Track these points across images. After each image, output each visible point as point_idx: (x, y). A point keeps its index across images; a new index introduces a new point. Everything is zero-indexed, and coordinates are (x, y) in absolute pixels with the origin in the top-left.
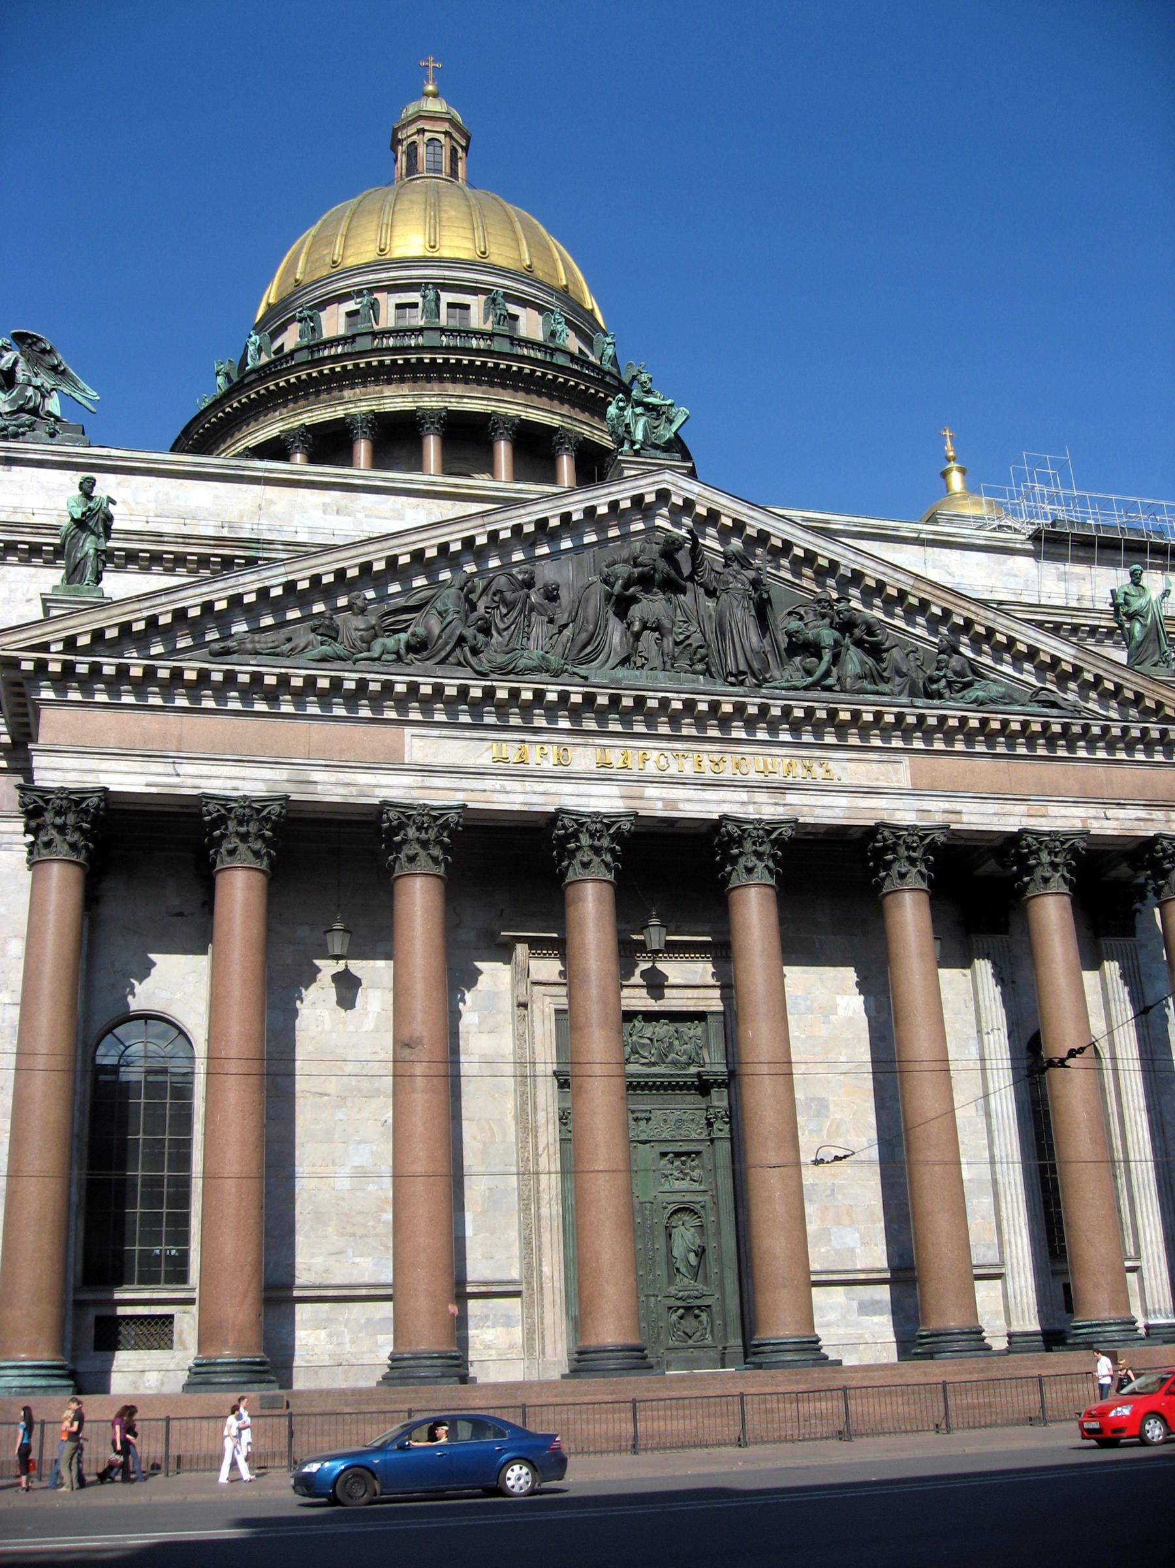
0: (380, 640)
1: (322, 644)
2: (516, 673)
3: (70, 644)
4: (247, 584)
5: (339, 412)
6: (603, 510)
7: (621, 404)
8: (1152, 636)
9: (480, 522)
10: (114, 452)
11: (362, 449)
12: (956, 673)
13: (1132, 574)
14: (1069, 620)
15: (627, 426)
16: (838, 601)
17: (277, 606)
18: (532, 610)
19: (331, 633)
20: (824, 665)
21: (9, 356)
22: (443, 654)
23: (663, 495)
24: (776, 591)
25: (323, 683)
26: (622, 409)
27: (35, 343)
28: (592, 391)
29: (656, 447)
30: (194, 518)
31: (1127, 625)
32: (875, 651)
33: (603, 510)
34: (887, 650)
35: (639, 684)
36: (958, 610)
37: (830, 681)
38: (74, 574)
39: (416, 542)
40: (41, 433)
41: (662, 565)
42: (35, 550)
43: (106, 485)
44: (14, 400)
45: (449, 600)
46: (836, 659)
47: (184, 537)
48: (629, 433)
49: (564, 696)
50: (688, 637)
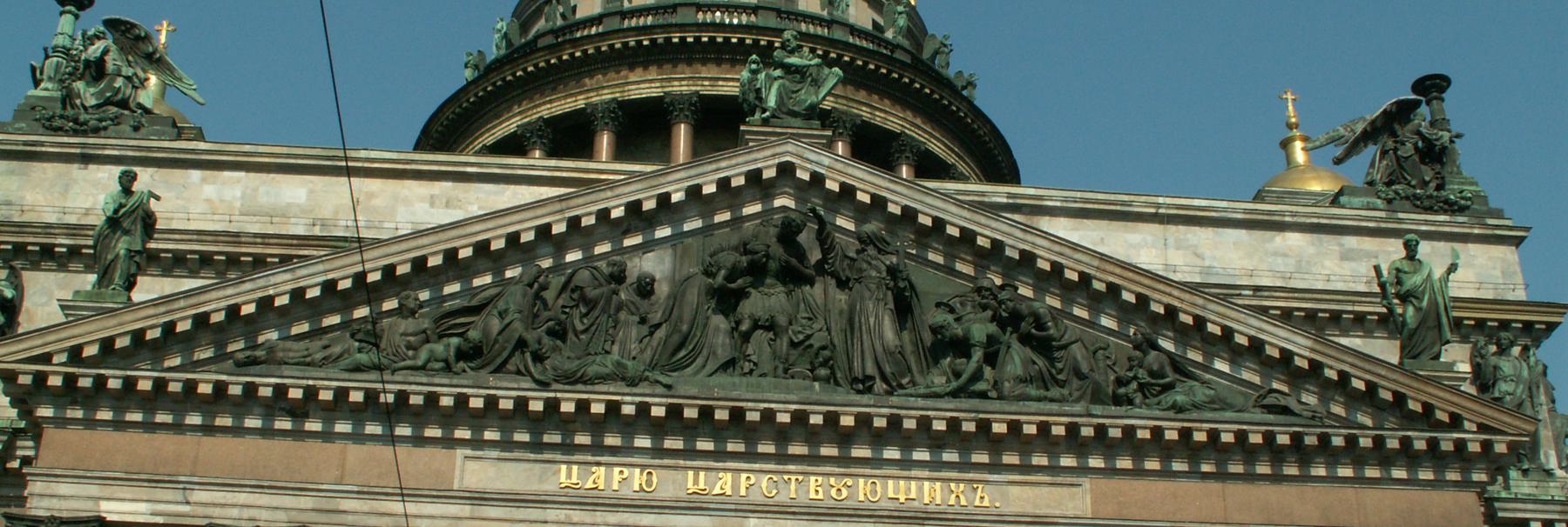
0: (428, 346)
1: (360, 350)
2: (585, 383)
4: (279, 284)
5: (580, 102)
7: (754, 66)
8: (1431, 323)
9: (558, 207)
11: (605, 141)
12: (1152, 374)
13: (1407, 245)
14: (1350, 308)
15: (758, 91)
16: (1002, 287)
17: (314, 309)
18: (619, 309)
19: (370, 335)
20: (973, 365)
21: (99, 46)
22: (499, 361)
23: (786, 170)
24: (923, 280)
26: (755, 72)
27: (128, 30)
28: (872, 67)
30: (283, 216)
31: (1399, 311)
32: (1043, 345)
33: (710, 189)
34: (1065, 347)
35: (735, 394)
36: (1156, 296)
37: (981, 386)
38: (104, 278)
40: (125, 128)
41: (778, 250)
43: (146, 179)
44: (102, 92)
45: (515, 300)
46: (991, 359)
47: (264, 236)
48: (760, 99)
49: (643, 409)
50: (808, 337)
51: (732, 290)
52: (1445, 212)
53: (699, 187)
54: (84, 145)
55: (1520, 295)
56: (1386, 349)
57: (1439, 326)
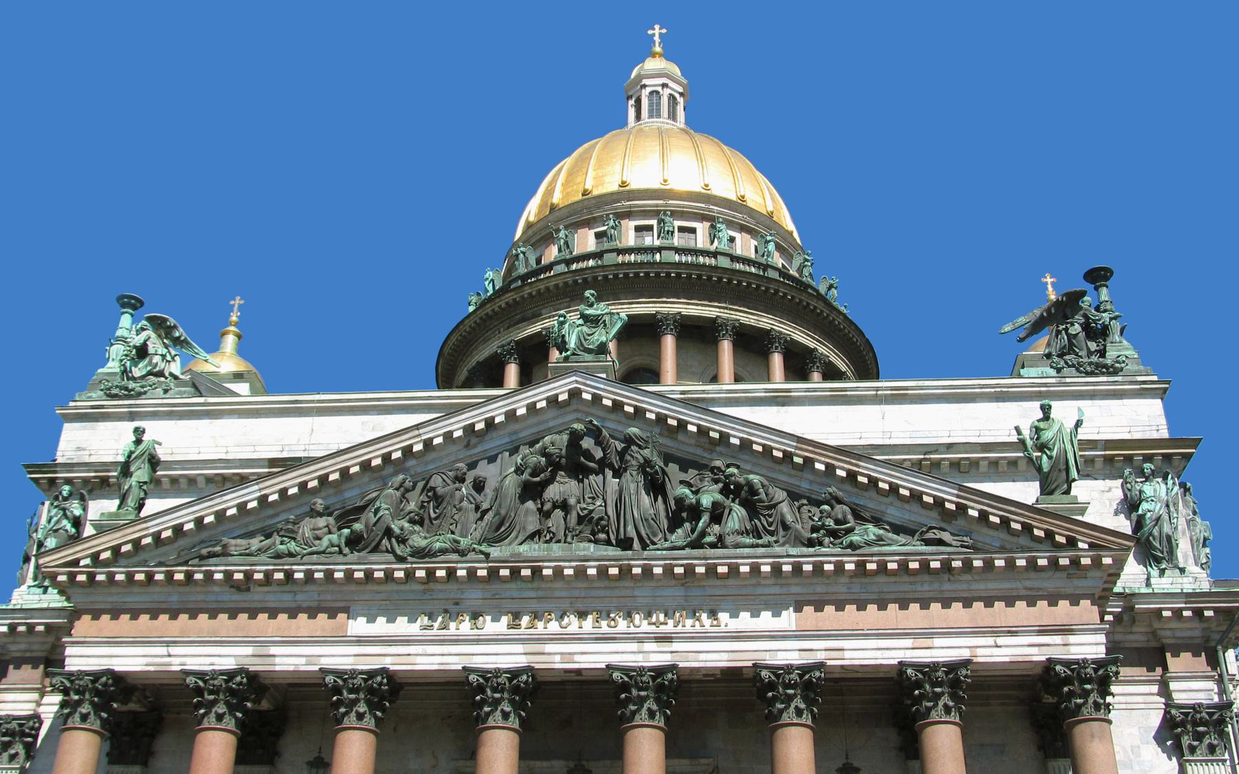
1: (282, 543)
3: (95, 557)
4: (229, 502)
12: (837, 522)
13: (1042, 407)
15: (563, 336)
21: (144, 335)
22: (373, 544)
23: (575, 394)
25: (279, 576)
33: (521, 411)
37: (708, 539)
39: (363, 455)
40: (160, 391)
52: (1103, 374)
54: (130, 406)
55: (1165, 434)
56: (1026, 492)
57: (1067, 470)
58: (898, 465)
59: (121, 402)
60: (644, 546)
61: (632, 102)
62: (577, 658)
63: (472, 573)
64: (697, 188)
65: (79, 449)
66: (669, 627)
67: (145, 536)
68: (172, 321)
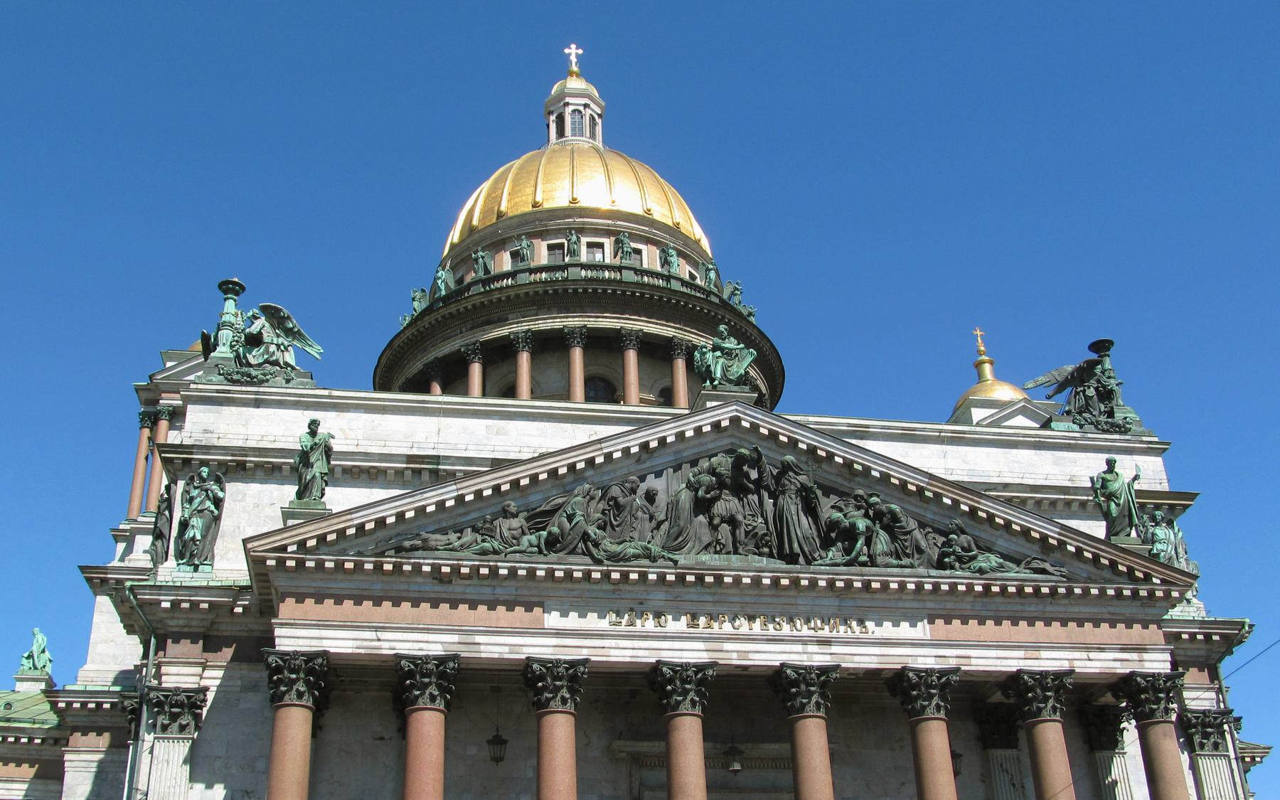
1: (483, 541)
6: (689, 434)
10: (336, 393)
12: (963, 549)
22: (572, 547)
23: (735, 421)
29: (730, 381)
39: (551, 463)
40: (280, 380)
42: (276, 468)
46: (868, 542)
51: (708, 499)
52: (1116, 432)
53: (683, 433)
55: (1165, 487)
56: (1098, 529)
58: (1009, 501)
59: (244, 389)
60: (809, 562)
61: (553, 118)
62: (751, 656)
63: (662, 577)
64: (639, 211)
65: (206, 431)
66: (826, 632)
67: (349, 527)
68: (286, 312)
